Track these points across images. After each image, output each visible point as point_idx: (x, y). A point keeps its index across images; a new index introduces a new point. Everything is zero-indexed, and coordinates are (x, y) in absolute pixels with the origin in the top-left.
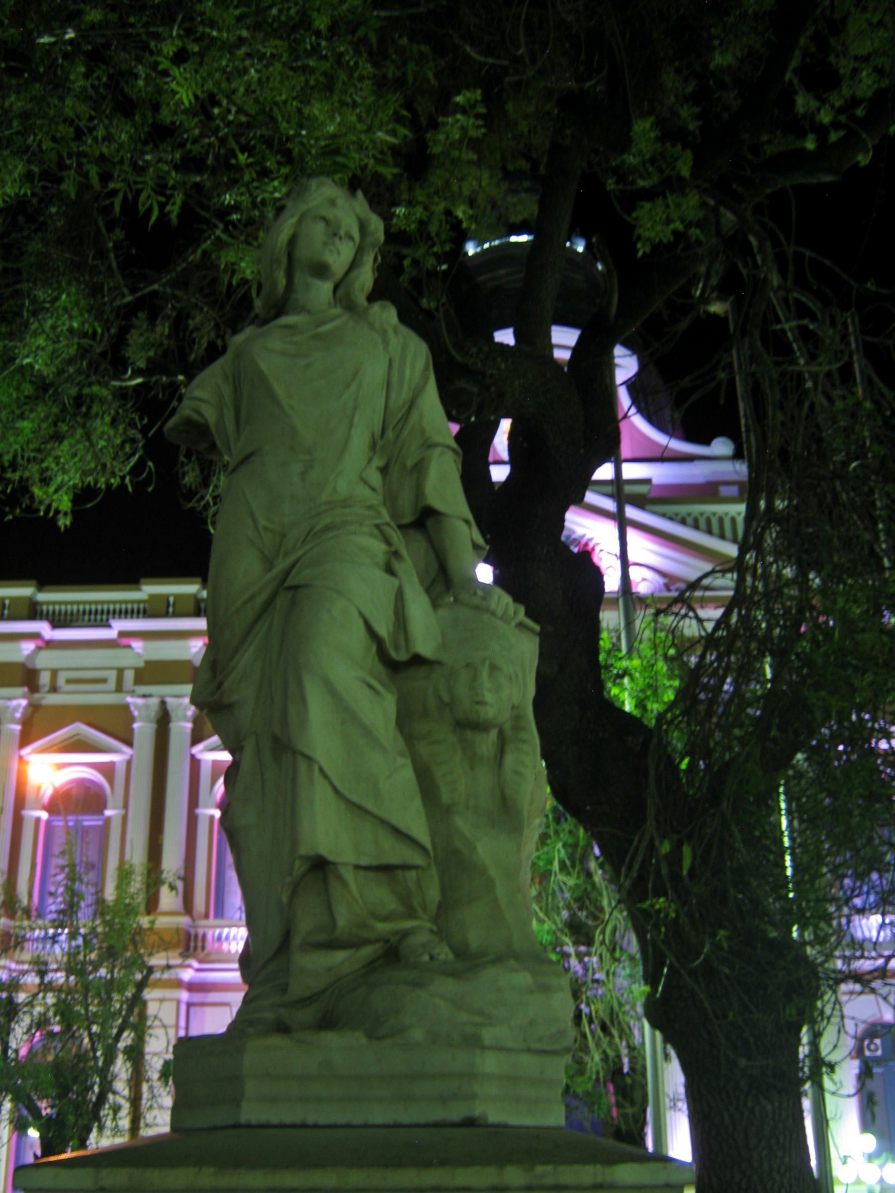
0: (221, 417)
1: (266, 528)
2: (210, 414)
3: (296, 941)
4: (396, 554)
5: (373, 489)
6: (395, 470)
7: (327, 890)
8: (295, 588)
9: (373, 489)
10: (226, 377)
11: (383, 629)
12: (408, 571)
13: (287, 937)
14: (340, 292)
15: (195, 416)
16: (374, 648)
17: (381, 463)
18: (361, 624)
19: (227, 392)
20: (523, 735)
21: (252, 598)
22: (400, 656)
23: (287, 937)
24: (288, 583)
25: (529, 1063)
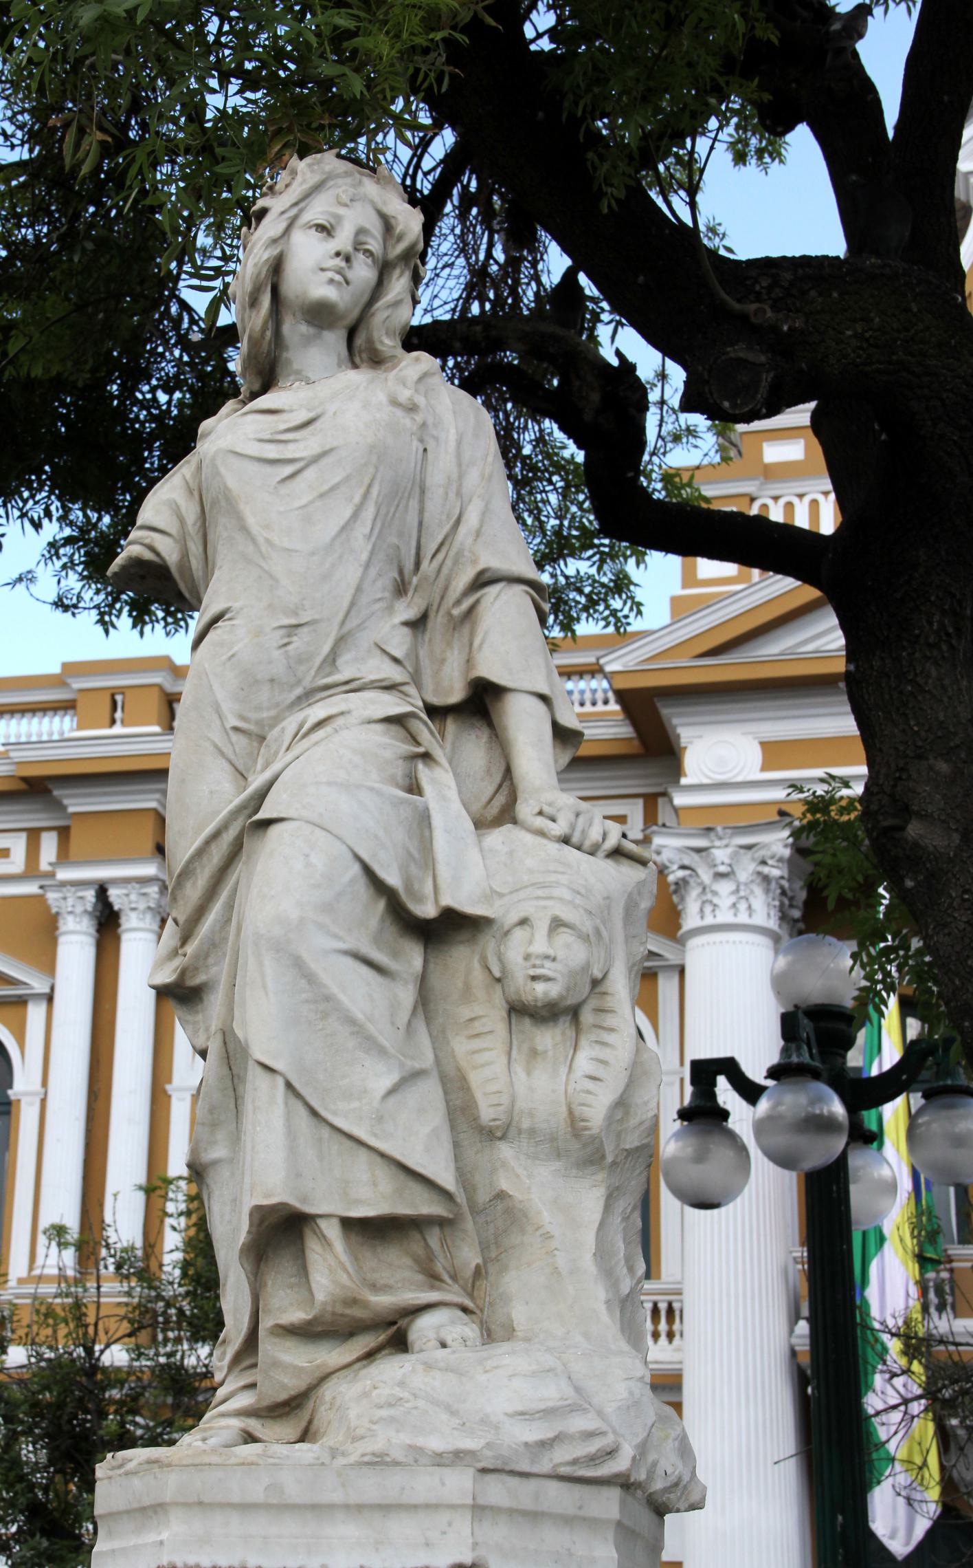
0: (185, 555)
1: (236, 729)
2: (169, 551)
3: (265, 1324)
4: (426, 757)
5: (396, 660)
6: (437, 622)
8: (267, 823)
9: (396, 660)
10: (191, 492)
11: (392, 878)
14: (359, 341)
15: (148, 555)
16: (381, 904)
17: (411, 613)
18: (356, 868)
19: (191, 512)
20: (610, 1021)
21: (216, 835)
22: (428, 911)
24: (262, 815)
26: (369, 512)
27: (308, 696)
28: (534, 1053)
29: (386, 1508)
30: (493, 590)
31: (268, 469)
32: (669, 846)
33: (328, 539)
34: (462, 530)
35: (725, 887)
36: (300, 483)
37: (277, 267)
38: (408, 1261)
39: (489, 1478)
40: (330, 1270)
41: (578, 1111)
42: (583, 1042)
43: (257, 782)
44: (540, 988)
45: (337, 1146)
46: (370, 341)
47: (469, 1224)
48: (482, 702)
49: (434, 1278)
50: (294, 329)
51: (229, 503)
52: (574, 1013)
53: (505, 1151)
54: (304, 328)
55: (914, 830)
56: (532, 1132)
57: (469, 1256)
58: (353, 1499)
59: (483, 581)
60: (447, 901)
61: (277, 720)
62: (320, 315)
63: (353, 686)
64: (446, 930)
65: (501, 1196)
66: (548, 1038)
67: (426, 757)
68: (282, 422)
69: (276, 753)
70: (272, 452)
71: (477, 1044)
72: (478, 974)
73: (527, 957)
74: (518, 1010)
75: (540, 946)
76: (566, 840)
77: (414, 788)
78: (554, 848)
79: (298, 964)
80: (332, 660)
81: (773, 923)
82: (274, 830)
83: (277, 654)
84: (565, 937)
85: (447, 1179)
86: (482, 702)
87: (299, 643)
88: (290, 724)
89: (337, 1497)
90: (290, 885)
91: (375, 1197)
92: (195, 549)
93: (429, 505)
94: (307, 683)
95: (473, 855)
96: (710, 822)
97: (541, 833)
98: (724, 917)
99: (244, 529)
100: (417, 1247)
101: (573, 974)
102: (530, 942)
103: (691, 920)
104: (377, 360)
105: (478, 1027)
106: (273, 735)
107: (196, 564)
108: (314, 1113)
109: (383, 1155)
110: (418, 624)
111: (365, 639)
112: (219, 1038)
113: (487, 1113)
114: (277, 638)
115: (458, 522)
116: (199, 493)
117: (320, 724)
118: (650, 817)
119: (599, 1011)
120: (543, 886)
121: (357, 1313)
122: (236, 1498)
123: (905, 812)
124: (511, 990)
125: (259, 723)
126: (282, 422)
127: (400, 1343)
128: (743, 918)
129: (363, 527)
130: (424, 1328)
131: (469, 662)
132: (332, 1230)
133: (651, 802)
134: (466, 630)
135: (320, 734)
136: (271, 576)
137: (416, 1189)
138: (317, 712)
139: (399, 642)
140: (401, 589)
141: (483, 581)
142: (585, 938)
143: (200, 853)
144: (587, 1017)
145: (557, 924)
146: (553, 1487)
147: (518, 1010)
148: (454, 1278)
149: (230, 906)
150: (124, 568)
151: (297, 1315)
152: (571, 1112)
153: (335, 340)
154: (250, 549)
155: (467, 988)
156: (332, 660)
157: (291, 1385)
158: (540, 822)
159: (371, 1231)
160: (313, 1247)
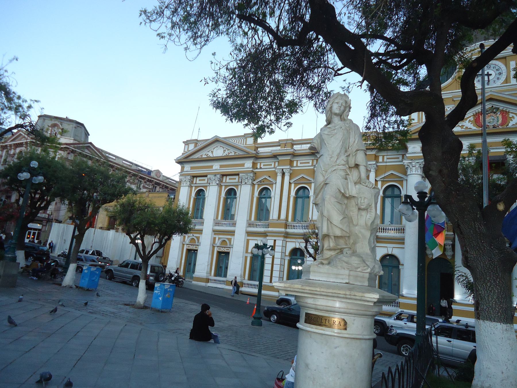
3: (324, 248)
11: (343, 191)
14: (342, 117)
20: (372, 211)
22: (348, 195)
25: (361, 274)
28: (361, 215)
32: (406, 162)
35: (414, 168)
37: (331, 107)
48: (357, 166)
52: (367, 209)
53: (357, 227)
55: (431, 172)
59: (357, 150)
62: (336, 114)
64: (350, 198)
66: (364, 213)
74: (359, 209)
77: (346, 179)
80: (336, 161)
81: (421, 174)
85: (348, 231)
86: (357, 166)
87: (332, 160)
93: (350, 140)
96: (412, 159)
98: (414, 173)
103: (409, 173)
107: (320, 148)
108: (331, 222)
111: (341, 159)
118: (403, 158)
123: (430, 170)
128: (417, 173)
132: (333, 237)
133: (403, 155)
137: (344, 232)
140: (346, 151)
141: (357, 150)
144: (369, 210)
145: (365, 198)
146: (359, 273)
147: (359, 209)
151: (328, 248)
153: (339, 117)
156: (336, 161)
157: (328, 256)
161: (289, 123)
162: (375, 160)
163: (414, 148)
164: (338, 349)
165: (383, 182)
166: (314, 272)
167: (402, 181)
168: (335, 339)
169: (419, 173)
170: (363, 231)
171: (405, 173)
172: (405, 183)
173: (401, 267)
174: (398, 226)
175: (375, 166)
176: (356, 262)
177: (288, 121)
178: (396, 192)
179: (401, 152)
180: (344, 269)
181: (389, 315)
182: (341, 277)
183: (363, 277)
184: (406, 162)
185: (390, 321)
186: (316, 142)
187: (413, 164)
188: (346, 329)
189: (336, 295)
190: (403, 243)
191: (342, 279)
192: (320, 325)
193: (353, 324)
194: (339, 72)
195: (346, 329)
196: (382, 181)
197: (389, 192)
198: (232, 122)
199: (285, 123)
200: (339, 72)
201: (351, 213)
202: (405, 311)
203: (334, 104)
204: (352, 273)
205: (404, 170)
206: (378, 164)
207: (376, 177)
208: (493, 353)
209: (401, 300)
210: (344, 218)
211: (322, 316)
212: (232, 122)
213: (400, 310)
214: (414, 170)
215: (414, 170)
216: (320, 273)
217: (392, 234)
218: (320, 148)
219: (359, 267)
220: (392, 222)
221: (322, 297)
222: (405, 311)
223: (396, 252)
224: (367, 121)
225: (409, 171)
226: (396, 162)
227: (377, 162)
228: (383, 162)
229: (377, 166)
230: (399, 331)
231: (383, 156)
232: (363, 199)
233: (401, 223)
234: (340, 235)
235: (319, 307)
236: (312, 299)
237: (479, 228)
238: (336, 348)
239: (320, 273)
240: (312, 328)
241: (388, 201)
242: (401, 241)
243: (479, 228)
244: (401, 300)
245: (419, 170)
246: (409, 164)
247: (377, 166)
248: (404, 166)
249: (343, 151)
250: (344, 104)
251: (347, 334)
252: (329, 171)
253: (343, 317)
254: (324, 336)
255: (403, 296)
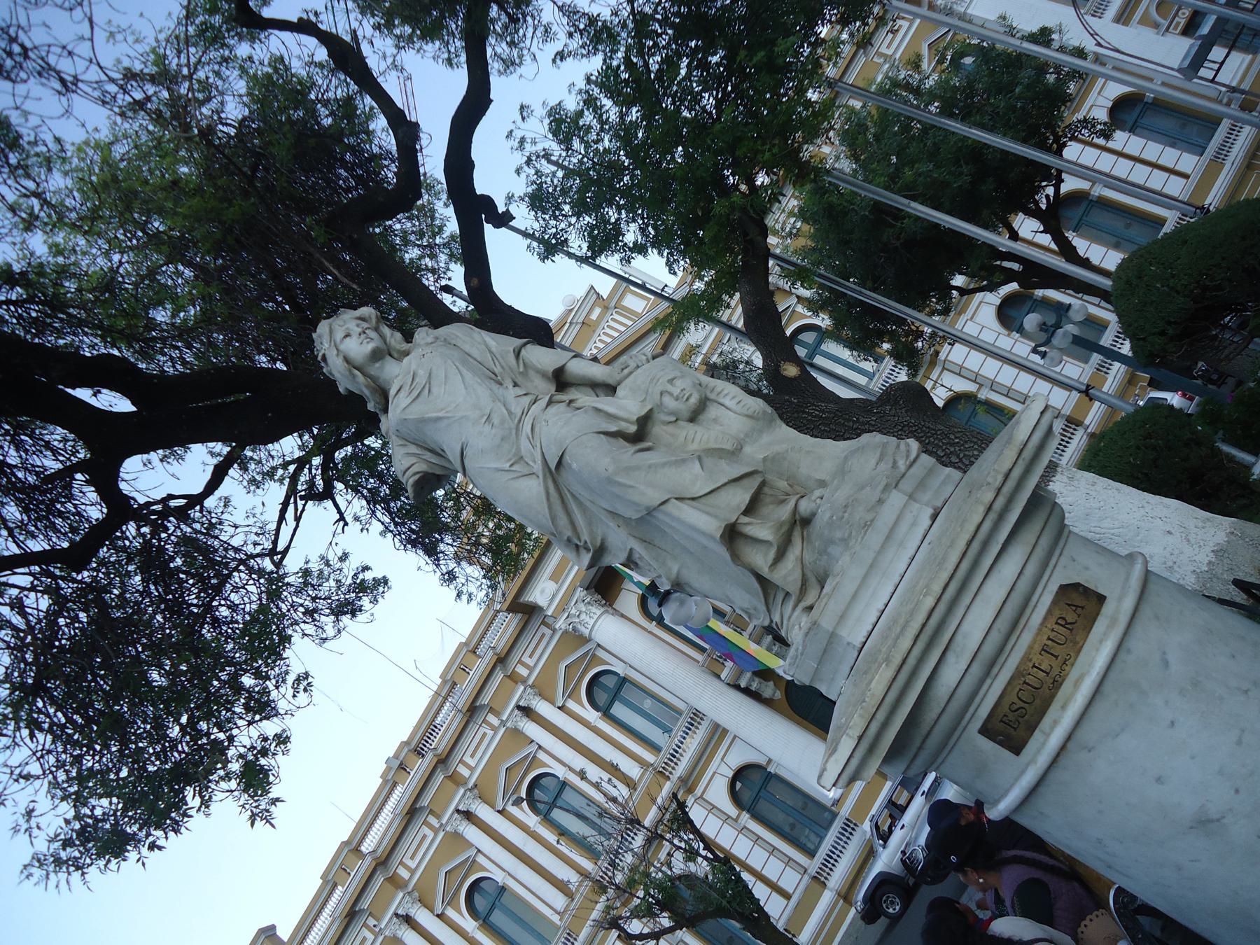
2: (421, 467)
3: (765, 572)
4: (571, 401)
6: (519, 380)
7: (747, 537)
8: (560, 463)
11: (613, 429)
12: (585, 399)
13: (760, 579)
14: (395, 355)
15: (417, 477)
22: (633, 429)
23: (760, 579)
24: (553, 467)
26: (464, 371)
27: (517, 429)
28: (715, 420)
29: (888, 537)
30: (523, 352)
31: (420, 399)
32: (561, 624)
33: (464, 391)
34: (494, 350)
35: (583, 616)
36: (434, 390)
37: (346, 360)
38: (771, 507)
39: (900, 486)
40: (761, 530)
41: (750, 412)
42: (721, 401)
43: (538, 467)
44: (693, 400)
45: (710, 499)
46: (399, 352)
47: (769, 477)
48: (561, 381)
49: (783, 502)
50: (374, 369)
51: (423, 421)
53: (748, 449)
54: (377, 365)
56: (747, 435)
57: (783, 484)
58: (877, 548)
59: (517, 354)
60: (635, 418)
61: (518, 449)
62: (376, 355)
63: (525, 413)
65: (765, 459)
66: (713, 411)
67: (571, 401)
68: (406, 388)
69: (532, 455)
70: (415, 393)
71: (697, 440)
72: (670, 428)
73: (677, 399)
75: (676, 391)
76: (638, 367)
78: (639, 370)
79: (629, 470)
80: (510, 413)
82: (567, 458)
83: (493, 431)
84: (678, 383)
87: (496, 420)
88: (524, 444)
89: (872, 555)
90: (595, 458)
91: (741, 497)
92: (428, 456)
94: (513, 426)
95: (624, 401)
96: (562, 608)
97: (631, 373)
98: (592, 622)
99: (439, 419)
100: (768, 500)
101: (694, 385)
102: (671, 394)
103: (586, 632)
104: (407, 353)
105: (690, 437)
106: (523, 452)
108: (693, 499)
109: (725, 484)
110: (516, 385)
112: (631, 539)
113: (728, 446)
114: (487, 428)
115: (490, 351)
116: (407, 440)
117: (532, 429)
119: (712, 391)
120: (652, 379)
121: (785, 529)
122: (848, 599)
124: (687, 415)
125: (515, 455)
126: (406, 388)
127: (806, 522)
129: (468, 375)
130: (805, 507)
131: (543, 375)
132: (745, 519)
133: (544, 623)
134: (531, 373)
135: (537, 430)
136: (462, 418)
137: (745, 482)
138: (527, 428)
139: (519, 391)
140: (501, 384)
141: (517, 354)
142: (682, 377)
143: (550, 508)
144: (712, 396)
145: (671, 381)
146: (912, 471)
147: (694, 418)
148: (788, 494)
149: (580, 504)
150: (415, 491)
151: (772, 554)
152: (747, 416)
154: (446, 421)
155: (672, 435)
156: (510, 413)
157: (797, 575)
158: (626, 371)
159: (750, 510)
160: (749, 530)
161: (298, 680)
162: (516, 683)
163: (542, 591)
164: (1171, 658)
165: (573, 695)
166: (842, 617)
167: (594, 655)
168: (1129, 651)
169: (599, 612)
170: (765, 438)
171: (585, 640)
172: (601, 654)
173: (771, 769)
174: (682, 722)
175: (529, 690)
176: (873, 462)
177: (290, 679)
178: (609, 682)
179: (536, 622)
180: (880, 502)
181: (869, 855)
182: (903, 527)
183: (930, 472)
184: (561, 624)
185: (886, 860)
186: (413, 460)
187: (573, 612)
188: (1101, 599)
189: (976, 545)
190: (725, 731)
191: (914, 524)
192: (1057, 684)
193: (1087, 568)
194: (280, 547)
195: (1101, 599)
196: (569, 696)
197: (602, 698)
198: (160, 848)
199: (291, 691)
200: (280, 547)
201: (694, 446)
202: (873, 812)
203: (342, 347)
204: (907, 485)
205: (575, 638)
206: (530, 682)
207: (553, 704)
208: (1116, 531)
209: (845, 811)
210: (700, 458)
211: (1026, 658)
212: (160, 848)
213: (867, 826)
214: (587, 619)
215: (587, 619)
216: (855, 596)
217: (692, 745)
218: (434, 459)
219: (895, 462)
220: (667, 730)
221: (960, 612)
222: (873, 812)
223: (737, 758)
224: (431, 567)
225: (582, 629)
226: (548, 643)
227: (524, 681)
228: (531, 669)
229: (532, 687)
230: (922, 840)
231: (520, 662)
232: (669, 388)
233: (680, 713)
234: (746, 498)
235: (989, 649)
236: (951, 657)
237: (823, 412)
238: (1166, 664)
239: (855, 596)
240: (1055, 723)
241: (618, 710)
242: (718, 733)
243: (823, 412)
244: (845, 811)
245: (594, 609)
246: (570, 620)
247: (532, 687)
248: (566, 632)
249: (495, 387)
250: (365, 325)
251: (1120, 599)
252: (524, 444)
253: (1053, 587)
254: (1107, 687)
255: (837, 802)
